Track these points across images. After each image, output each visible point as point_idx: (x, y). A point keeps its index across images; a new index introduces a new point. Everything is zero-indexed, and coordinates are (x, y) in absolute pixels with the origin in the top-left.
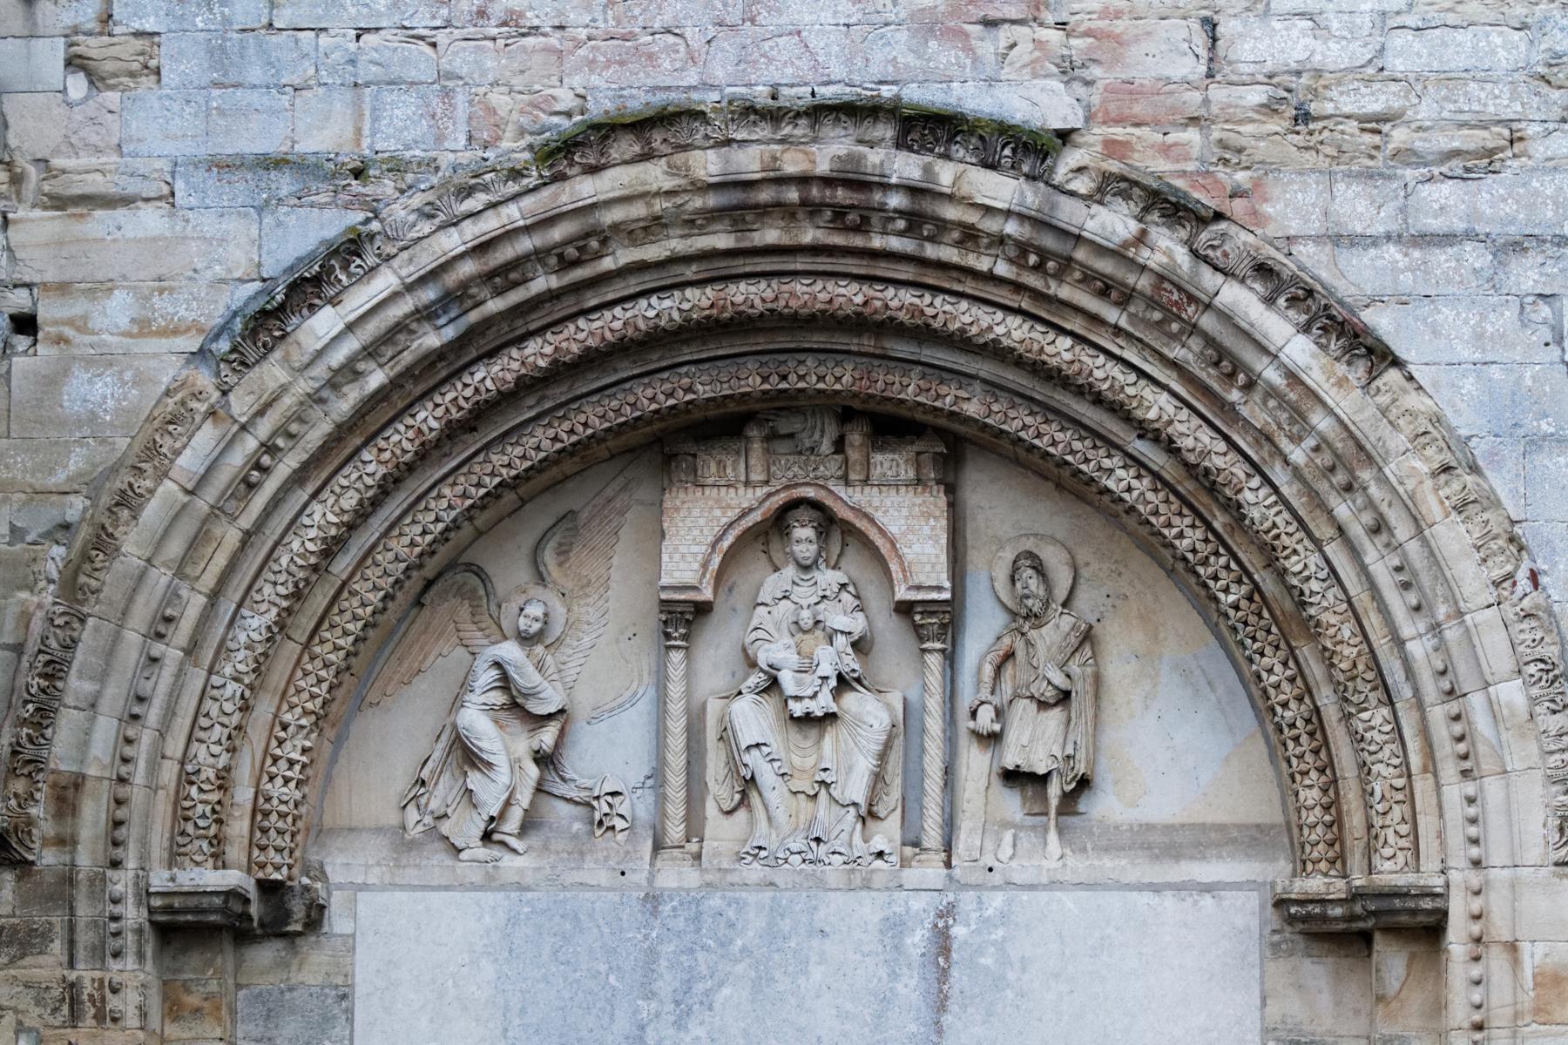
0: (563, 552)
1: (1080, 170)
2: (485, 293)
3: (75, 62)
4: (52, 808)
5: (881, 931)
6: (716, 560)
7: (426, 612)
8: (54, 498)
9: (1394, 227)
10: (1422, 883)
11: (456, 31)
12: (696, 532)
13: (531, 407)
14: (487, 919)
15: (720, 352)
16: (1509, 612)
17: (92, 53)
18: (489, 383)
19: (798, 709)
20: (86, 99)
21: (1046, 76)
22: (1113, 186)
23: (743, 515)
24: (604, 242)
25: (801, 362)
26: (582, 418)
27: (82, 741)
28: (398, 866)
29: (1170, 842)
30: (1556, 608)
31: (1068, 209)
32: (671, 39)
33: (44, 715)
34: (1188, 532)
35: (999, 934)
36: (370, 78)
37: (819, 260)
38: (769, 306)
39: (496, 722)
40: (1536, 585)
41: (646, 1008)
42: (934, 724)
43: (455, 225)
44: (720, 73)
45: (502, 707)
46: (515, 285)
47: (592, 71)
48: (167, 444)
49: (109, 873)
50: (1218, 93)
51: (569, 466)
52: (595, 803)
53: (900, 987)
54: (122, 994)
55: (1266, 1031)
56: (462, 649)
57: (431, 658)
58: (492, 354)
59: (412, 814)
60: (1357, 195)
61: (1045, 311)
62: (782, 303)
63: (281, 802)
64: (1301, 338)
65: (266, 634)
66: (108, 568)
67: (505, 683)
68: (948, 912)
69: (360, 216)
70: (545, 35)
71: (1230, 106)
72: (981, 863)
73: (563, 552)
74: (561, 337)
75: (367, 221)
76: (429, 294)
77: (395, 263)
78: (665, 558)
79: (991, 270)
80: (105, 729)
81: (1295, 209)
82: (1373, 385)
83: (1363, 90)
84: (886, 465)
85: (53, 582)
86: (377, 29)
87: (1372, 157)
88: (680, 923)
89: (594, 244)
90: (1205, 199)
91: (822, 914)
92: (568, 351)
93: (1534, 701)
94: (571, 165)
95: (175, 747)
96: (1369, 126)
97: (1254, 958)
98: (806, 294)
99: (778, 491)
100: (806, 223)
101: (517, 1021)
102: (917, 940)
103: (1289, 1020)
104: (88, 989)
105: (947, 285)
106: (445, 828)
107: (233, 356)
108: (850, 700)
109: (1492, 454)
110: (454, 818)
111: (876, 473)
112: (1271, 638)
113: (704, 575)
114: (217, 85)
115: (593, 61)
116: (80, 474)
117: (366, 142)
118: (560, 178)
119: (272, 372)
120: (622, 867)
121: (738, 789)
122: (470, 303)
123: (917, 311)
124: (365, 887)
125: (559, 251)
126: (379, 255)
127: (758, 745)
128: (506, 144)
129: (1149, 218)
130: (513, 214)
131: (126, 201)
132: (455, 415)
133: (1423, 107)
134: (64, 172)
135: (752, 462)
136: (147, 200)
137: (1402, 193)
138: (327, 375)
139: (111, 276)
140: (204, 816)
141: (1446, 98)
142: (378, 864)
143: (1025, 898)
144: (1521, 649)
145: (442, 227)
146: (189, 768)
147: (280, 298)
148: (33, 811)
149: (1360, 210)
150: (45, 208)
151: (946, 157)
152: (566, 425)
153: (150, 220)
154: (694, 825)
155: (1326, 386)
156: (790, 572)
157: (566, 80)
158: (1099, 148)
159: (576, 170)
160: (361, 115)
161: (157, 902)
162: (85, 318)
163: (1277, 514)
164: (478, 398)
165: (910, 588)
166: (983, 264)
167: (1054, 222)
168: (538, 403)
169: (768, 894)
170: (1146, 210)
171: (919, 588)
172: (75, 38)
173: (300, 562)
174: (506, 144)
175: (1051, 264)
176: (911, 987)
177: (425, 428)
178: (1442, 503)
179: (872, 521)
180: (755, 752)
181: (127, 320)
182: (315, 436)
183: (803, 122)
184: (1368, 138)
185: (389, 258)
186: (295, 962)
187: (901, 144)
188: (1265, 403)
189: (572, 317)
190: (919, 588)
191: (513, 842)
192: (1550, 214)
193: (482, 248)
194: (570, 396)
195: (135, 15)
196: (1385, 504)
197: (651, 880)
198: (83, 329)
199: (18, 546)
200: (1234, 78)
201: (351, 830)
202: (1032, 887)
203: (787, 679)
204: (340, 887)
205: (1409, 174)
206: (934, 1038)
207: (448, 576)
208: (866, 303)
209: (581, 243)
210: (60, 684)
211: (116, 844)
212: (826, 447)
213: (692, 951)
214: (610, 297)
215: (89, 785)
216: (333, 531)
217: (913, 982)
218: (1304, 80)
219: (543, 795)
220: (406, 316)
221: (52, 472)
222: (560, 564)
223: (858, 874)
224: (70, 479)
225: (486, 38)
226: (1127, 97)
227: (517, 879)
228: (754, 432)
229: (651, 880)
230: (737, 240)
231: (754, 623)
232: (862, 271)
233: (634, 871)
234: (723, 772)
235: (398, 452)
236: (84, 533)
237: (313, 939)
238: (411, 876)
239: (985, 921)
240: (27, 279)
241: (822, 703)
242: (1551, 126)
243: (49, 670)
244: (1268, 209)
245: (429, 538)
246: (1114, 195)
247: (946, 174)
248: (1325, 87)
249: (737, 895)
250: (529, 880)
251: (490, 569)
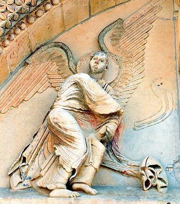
7: (29, 68)
39: (76, 118)
52: (143, 172)
56: (52, 89)
57: (32, 93)
59: (16, 178)
67: (82, 95)
73: (115, 39)
106: (39, 183)
110: (45, 177)
191: (88, 188)
207: (43, 48)
219: (106, 170)
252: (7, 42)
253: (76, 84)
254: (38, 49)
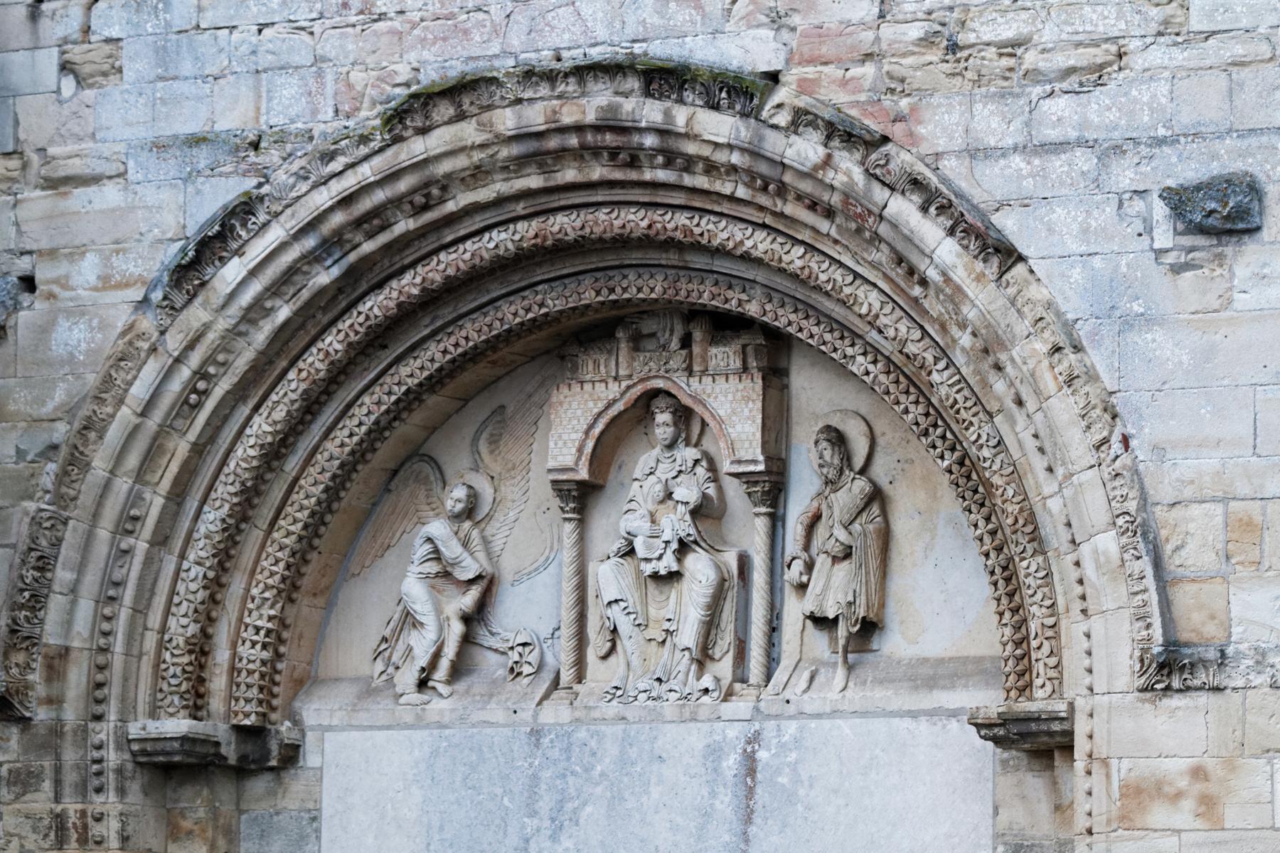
0: (494, 442)
1: (780, 106)
2: (359, 237)
3: (66, 67)
4: (44, 674)
5: (704, 757)
6: (590, 445)
7: (393, 497)
8: (45, 424)
9: (1020, 140)
10: (1050, 708)
11: (327, 21)
12: (575, 422)
13: (426, 326)
14: (417, 753)
15: (565, 272)
16: (1106, 471)
17: (77, 59)
18: (376, 310)
19: (648, 569)
20: (75, 95)
21: (758, 26)
22: (801, 119)
24: (444, 188)
25: (625, 277)
26: (464, 333)
27: (68, 620)
28: (353, 710)
29: (932, 674)
30: (1141, 467)
31: (771, 140)
32: (481, 16)
33: (37, 602)
34: (912, 408)
35: (793, 756)
36: (266, 65)
37: (614, 192)
38: (579, 233)
40: (1127, 447)
41: (531, 823)
42: (759, 577)
43: (324, 183)
44: (516, 42)
45: (437, 575)
46: (383, 228)
47: (423, 47)
48: (120, 377)
49: (91, 725)
50: (887, 31)
51: (481, 371)
53: (717, 803)
54: (105, 822)
55: (998, 836)
57: (398, 535)
58: (380, 285)
60: (992, 113)
61: (780, 227)
62: (588, 230)
63: (249, 661)
64: (949, 239)
65: (219, 526)
66: (83, 480)
67: (436, 555)
68: (755, 739)
69: (254, 182)
70: (391, 19)
71: (896, 42)
72: (781, 697)
74: (428, 268)
75: (260, 185)
76: (310, 242)
77: (282, 218)
78: (552, 444)
79: (733, 193)
80: (85, 608)
81: (945, 128)
82: (1003, 279)
83: (1000, 20)
84: (720, 357)
85: (48, 492)
86: (273, 24)
87: (1006, 79)
88: (555, 753)
89: (435, 191)
90: (875, 126)
91: (660, 742)
92: (433, 282)
93: (1124, 549)
94: (406, 128)
95: (155, 620)
96: (1005, 51)
97: (988, 773)
98: (604, 221)
99: (635, 384)
100: (593, 163)
101: (437, 837)
102: (731, 763)
103: (1015, 827)
104: (73, 818)
105: (709, 207)
107: (165, 303)
109: (1094, 334)
112: (977, 496)
113: (579, 458)
114: (161, 78)
115: (425, 39)
116: (62, 405)
117: (263, 119)
118: (398, 139)
119: (197, 315)
120: (515, 707)
122: (348, 246)
123: (687, 231)
124: (330, 728)
125: (409, 199)
126: (269, 213)
127: (616, 601)
128: (364, 114)
129: (832, 144)
130: (366, 172)
131: (95, 180)
132: (353, 338)
133: (1047, 31)
134: (54, 158)
135: (620, 359)
136: (110, 178)
137: (1027, 109)
138: (240, 314)
139: (85, 241)
140: (174, 676)
141: (1066, 23)
142: (340, 709)
143: (813, 725)
144: (1113, 504)
145: (315, 186)
146: (166, 637)
147: (191, 254)
148: (31, 677)
149: (994, 125)
150: (43, 189)
151: (681, 101)
152: (453, 340)
153: (110, 194)
155: (968, 281)
157: (405, 57)
158: (794, 87)
159: (410, 132)
160: (260, 97)
161: (135, 747)
162: (67, 277)
163: (958, 392)
164: (369, 323)
165: (732, 463)
166: (727, 189)
167: (762, 152)
168: (432, 322)
169: (621, 727)
170: (829, 137)
171: (739, 462)
172: (65, 47)
173: (244, 465)
174: (364, 114)
175: (771, 187)
176: (725, 803)
177: (331, 350)
178: (1056, 379)
180: (614, 606)
181: (94, 277)
182: (242, 362)
183: (572, 80)
184: (1005, 62)
185: (277, 215)
186: (281, 791)
187: (648, 93)
188: (938, 297)
189: (436, 252)
190: (739, 462)
192: (1146, 119)
193: (346, 201)
194: (455, 315)
195: (106, 24)
196: (1018, 381)
197: (535, 716)
198: (66, 287)
199: (22, 465)
200: (900, 17)
201: (336, 680)
202: (818, 716)
204: (312, 728)
205: (1038, 90)
206: (742, 846)
207: (407, 465)
208: (650, 226)
209: (425, 191)
210: (49, 575)
211: (99, 702)
212: (675, 344)
213: (564, 776)
214: (462, 232)
215: (73, 655)
216: (269, 439)
217: (727, 799)
218: (955, 15)
220: (296, 261)
221: (44, 403)
222: (492, 452)
224: (56, 409)
225: (347, 26)
226: (817, 40)
227: (437, 718)
229: (535, 716)
230: (546, 180)
232: (646, 199)
233: (523, 710)
235: (313, 371)
236: (64, 451)
237: (293, 771)
238: (362, 718)
239: (782, 746)
240: (28, 248)
241: (668, 563)
242: (1149, 40)
243: (40, 564)
244: (921, 130)
245: (355, 439)
246: (806, 126)
247: (681, 116)
248: (972, 20)
249: (598, 728)
250: (446, 720)
251: (441, 460)
252: (343, 494)
253: (429, 540)
254: (402, 464)
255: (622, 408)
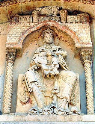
6: (23, 38)
23: (31, 27)
78: (8, 37)
108: (63, 73)
111: (69, 20)
113: (19, 41)
121: (27, 96)
127: (34, 82)
135: (34, 18)
154: (13, 109)
156: (45, 46)
171: (83, 43)
179: (69, 29)
180: (33, 84)
190: (83, 43)
203: (44, 66)
223: (67, 117)
228: (35, 12)
231: (34, 57)
234: (23, 92)
241: (55, 71)
255: (36, 29)
